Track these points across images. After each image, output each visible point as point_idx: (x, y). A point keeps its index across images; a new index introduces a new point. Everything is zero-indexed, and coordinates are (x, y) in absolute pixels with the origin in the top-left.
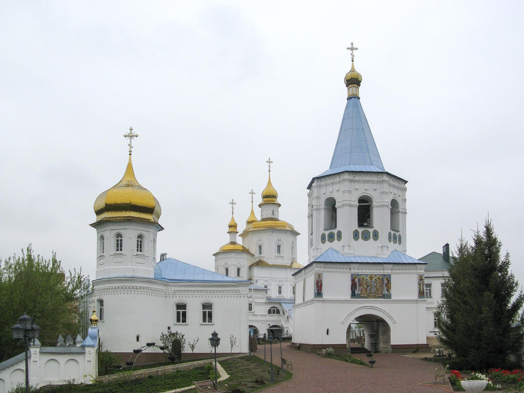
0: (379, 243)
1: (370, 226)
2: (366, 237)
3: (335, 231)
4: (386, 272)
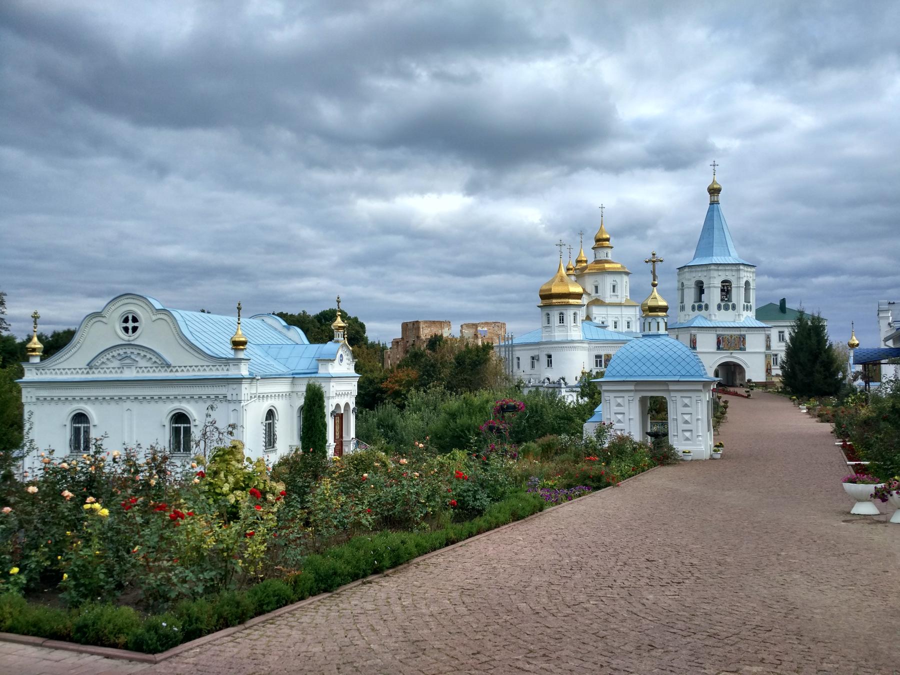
0: (735, 312)
1: (730, 300)
2: (726, 308)
3: (703, 304)
4: (742, 333)
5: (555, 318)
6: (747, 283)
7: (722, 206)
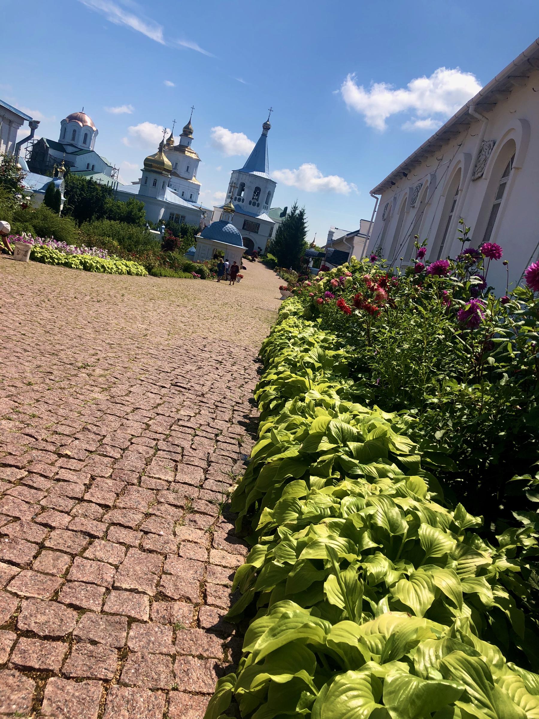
2: (254, 204)
5: (151, 182)
7: (268, 139)
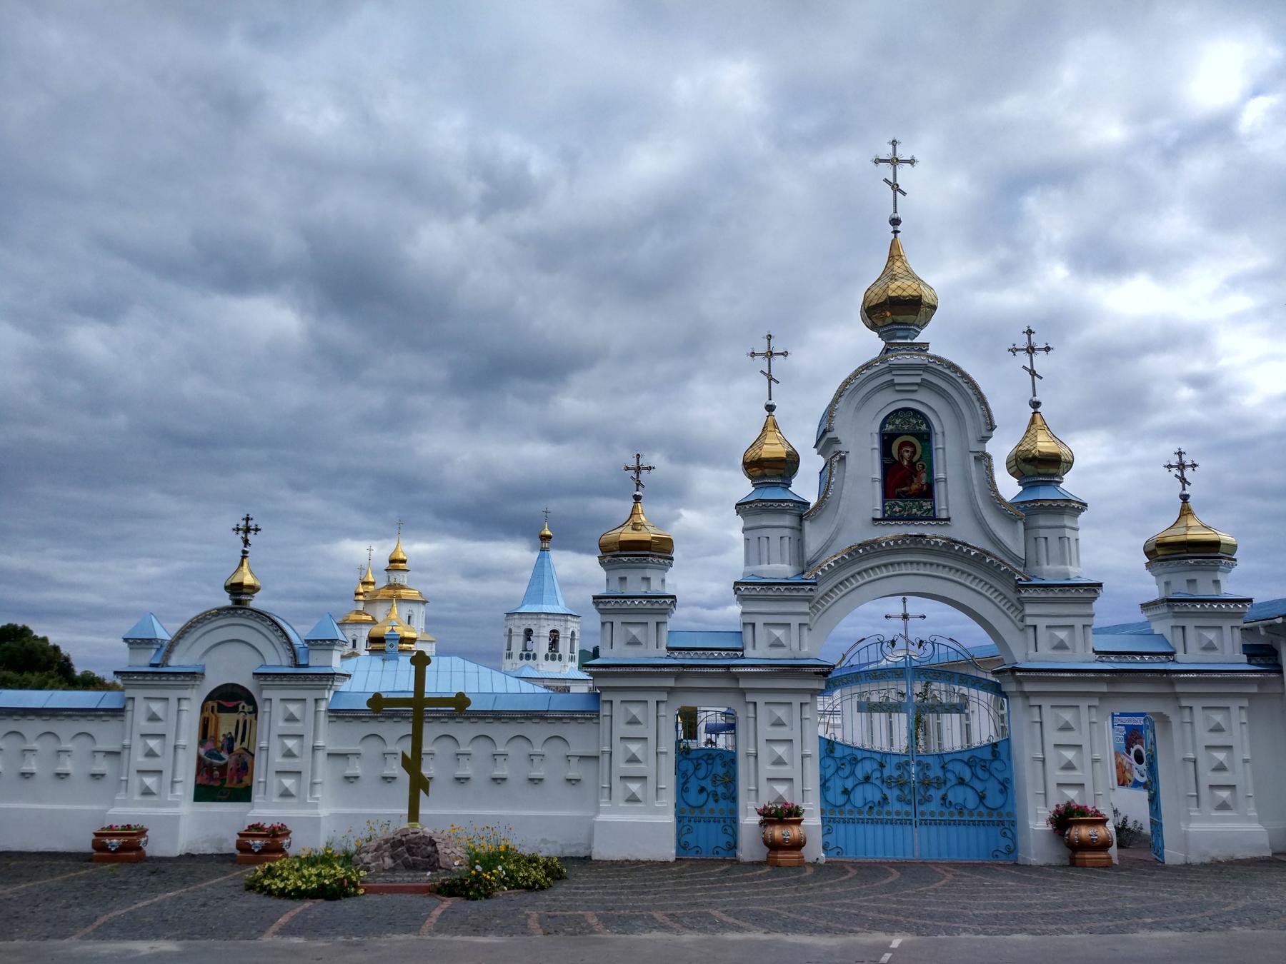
0: (561, 664)
2: (553, 659)
6: (573, 633)
